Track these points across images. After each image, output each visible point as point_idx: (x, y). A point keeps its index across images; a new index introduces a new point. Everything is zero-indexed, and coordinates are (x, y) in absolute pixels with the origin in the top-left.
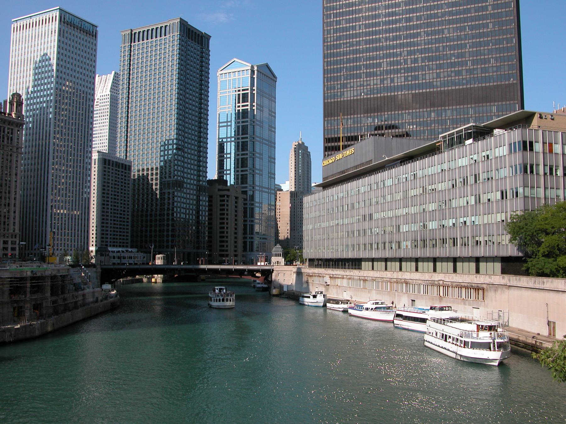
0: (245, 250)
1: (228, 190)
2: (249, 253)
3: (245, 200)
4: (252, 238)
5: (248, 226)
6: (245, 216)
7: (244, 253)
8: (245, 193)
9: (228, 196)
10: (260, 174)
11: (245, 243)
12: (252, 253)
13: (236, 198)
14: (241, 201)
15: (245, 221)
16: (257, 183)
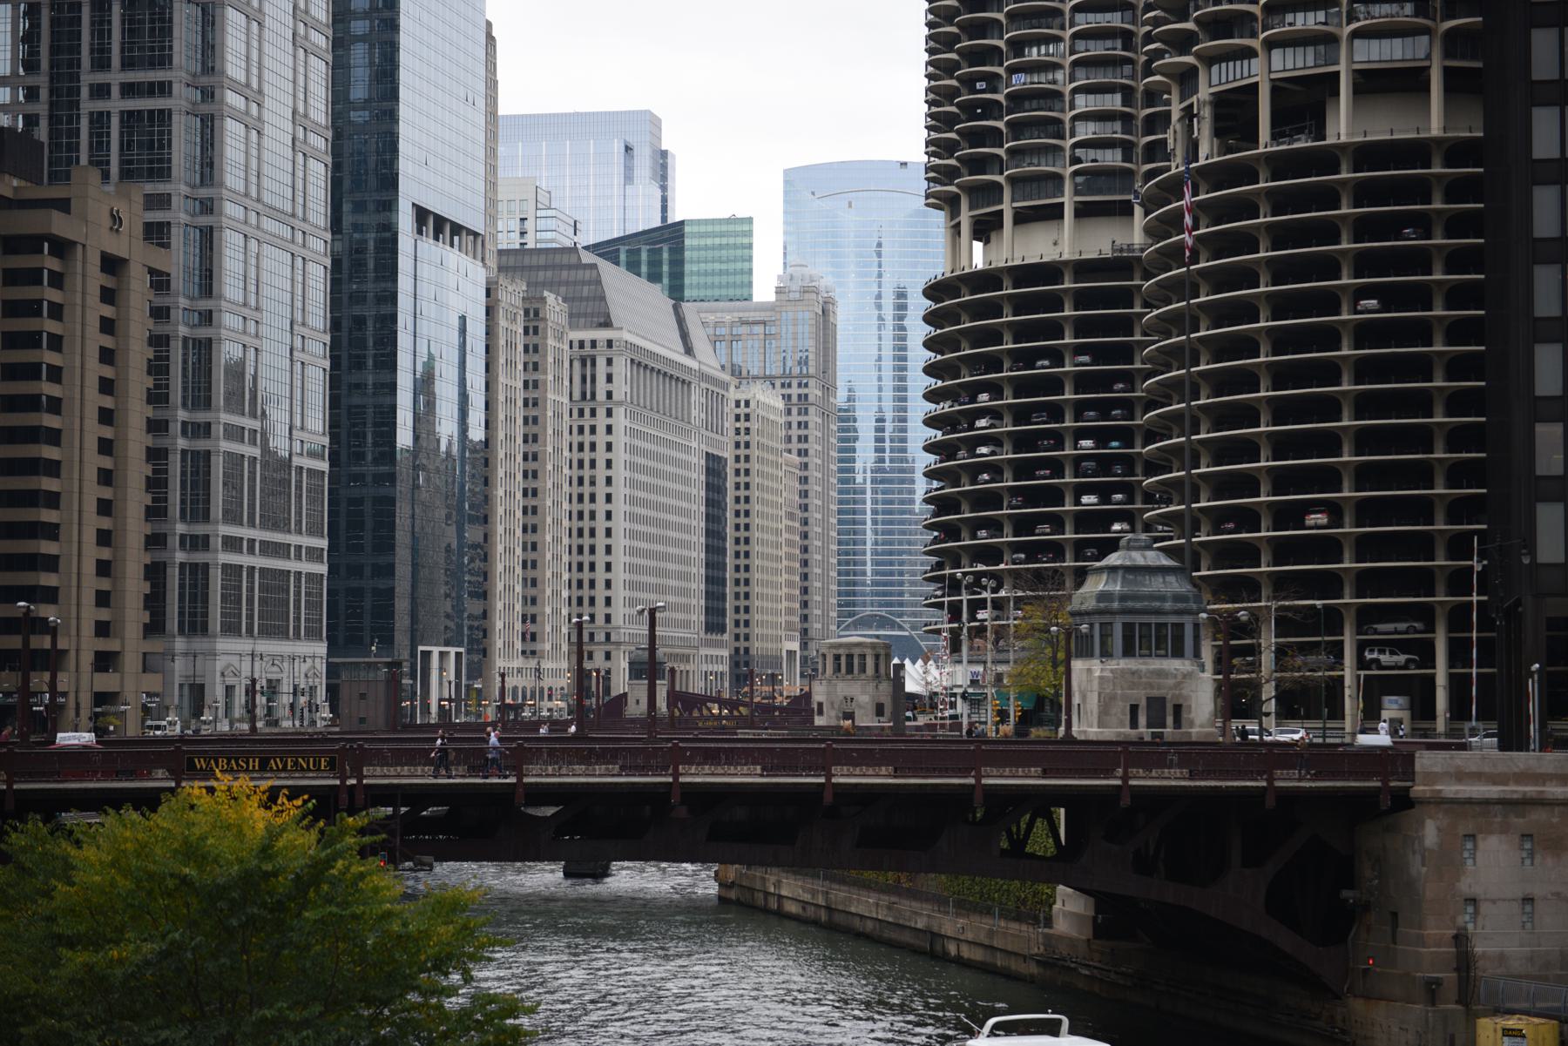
0: (155, 627)
1: (64, 205)
2: (180, 644)
3: (160, 281)
4: (199, 543)
5: (175, 466)
6: (157, 397)
7: (155, 645)
8: (157, 234)
9: (62, 248)
10: (242, 118)
11: (155, 573)
12: (199, 644)
13: (112, 264)
14: (138, 287)
15: (157, 427)
16: (233, 178)
